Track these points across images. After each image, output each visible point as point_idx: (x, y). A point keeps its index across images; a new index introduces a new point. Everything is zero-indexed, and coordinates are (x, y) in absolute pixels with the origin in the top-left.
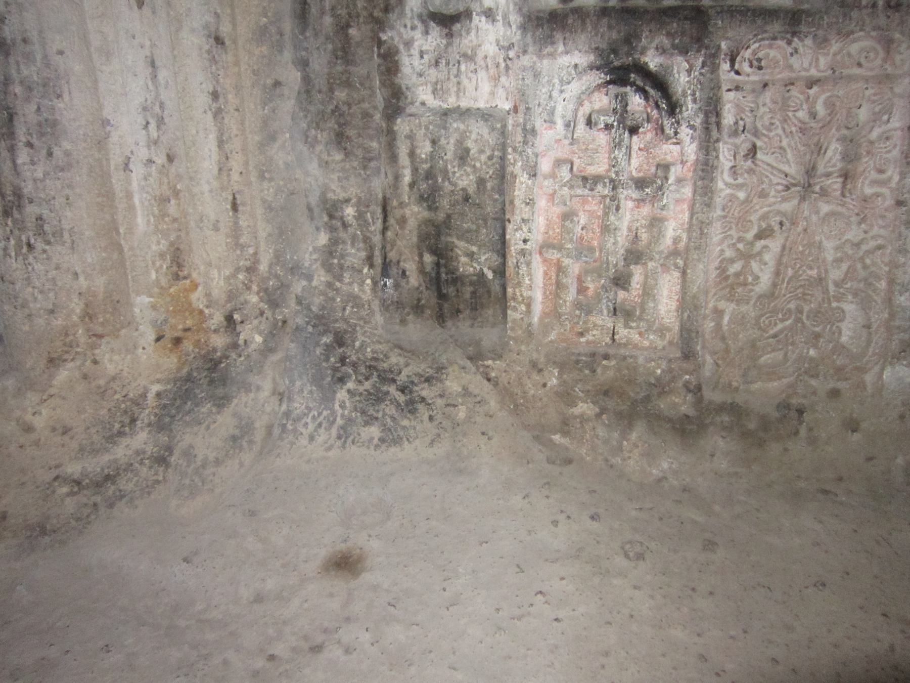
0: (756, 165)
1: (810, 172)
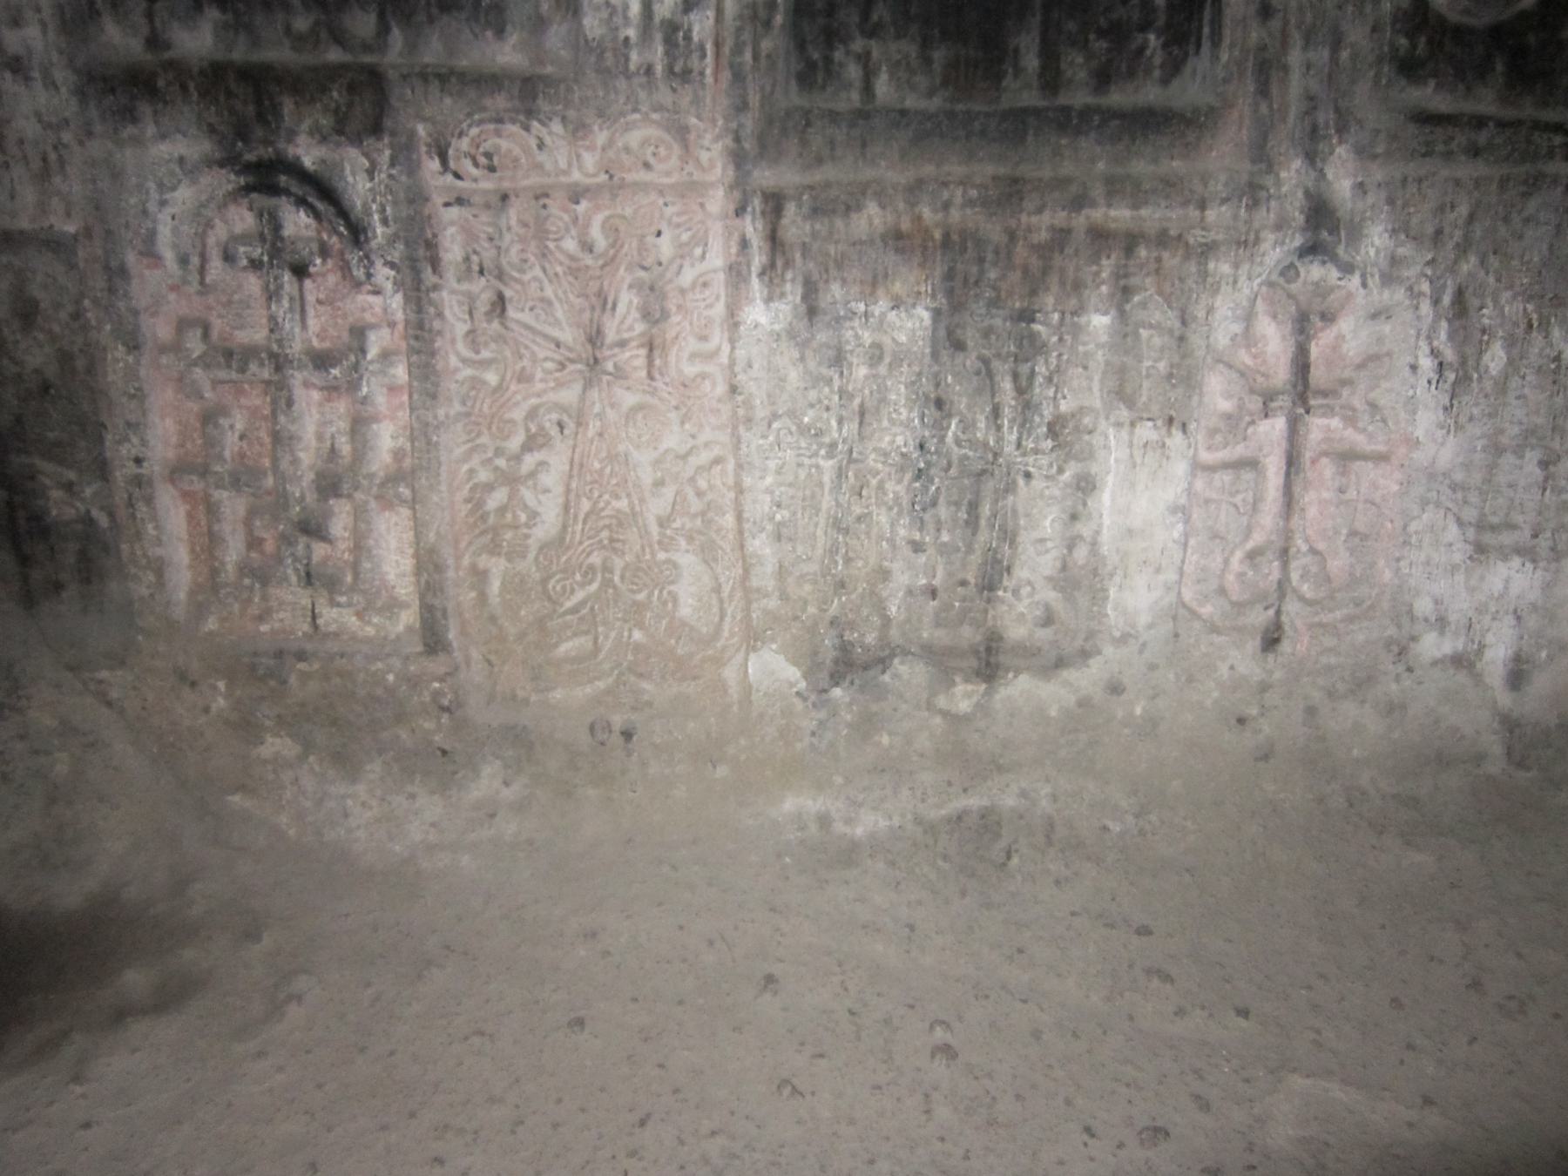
0: (506, 328)
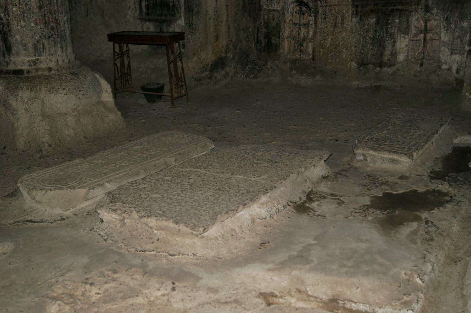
1: (335, 22)
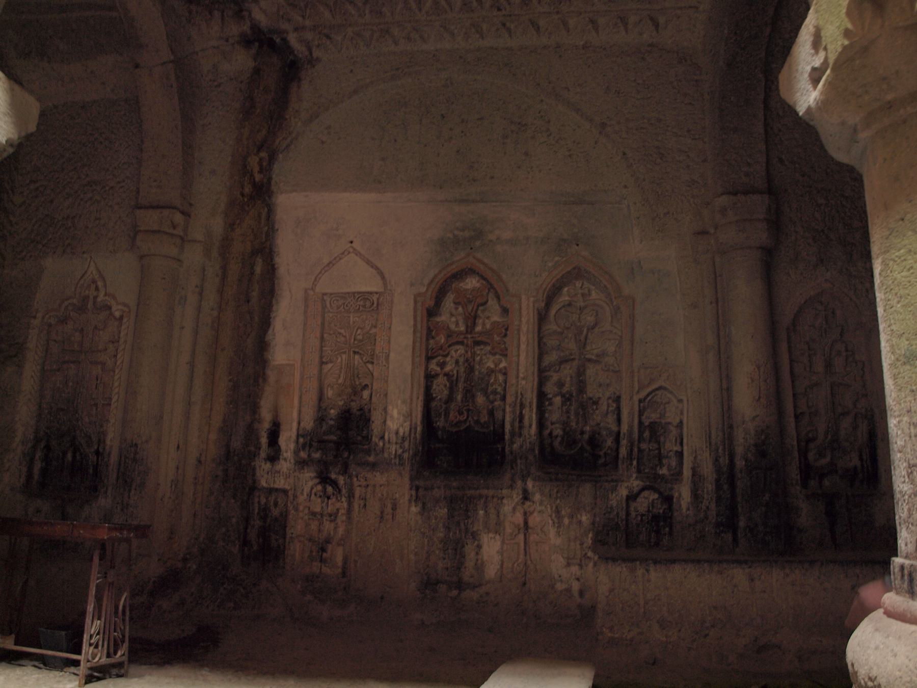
1: (382, 512)
